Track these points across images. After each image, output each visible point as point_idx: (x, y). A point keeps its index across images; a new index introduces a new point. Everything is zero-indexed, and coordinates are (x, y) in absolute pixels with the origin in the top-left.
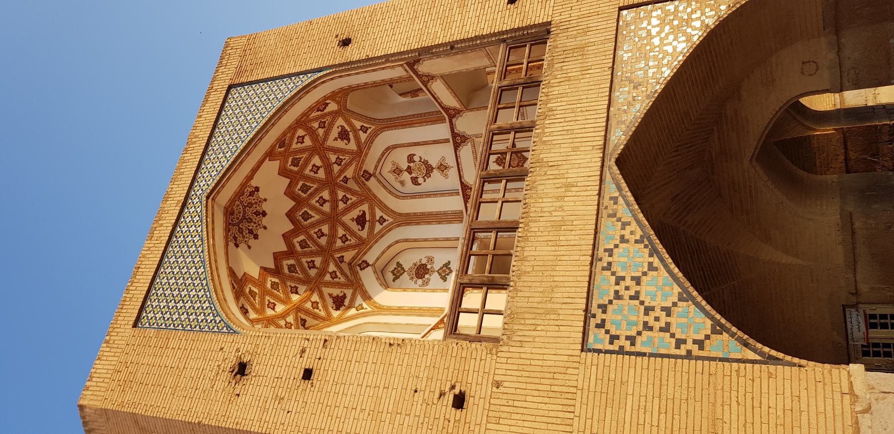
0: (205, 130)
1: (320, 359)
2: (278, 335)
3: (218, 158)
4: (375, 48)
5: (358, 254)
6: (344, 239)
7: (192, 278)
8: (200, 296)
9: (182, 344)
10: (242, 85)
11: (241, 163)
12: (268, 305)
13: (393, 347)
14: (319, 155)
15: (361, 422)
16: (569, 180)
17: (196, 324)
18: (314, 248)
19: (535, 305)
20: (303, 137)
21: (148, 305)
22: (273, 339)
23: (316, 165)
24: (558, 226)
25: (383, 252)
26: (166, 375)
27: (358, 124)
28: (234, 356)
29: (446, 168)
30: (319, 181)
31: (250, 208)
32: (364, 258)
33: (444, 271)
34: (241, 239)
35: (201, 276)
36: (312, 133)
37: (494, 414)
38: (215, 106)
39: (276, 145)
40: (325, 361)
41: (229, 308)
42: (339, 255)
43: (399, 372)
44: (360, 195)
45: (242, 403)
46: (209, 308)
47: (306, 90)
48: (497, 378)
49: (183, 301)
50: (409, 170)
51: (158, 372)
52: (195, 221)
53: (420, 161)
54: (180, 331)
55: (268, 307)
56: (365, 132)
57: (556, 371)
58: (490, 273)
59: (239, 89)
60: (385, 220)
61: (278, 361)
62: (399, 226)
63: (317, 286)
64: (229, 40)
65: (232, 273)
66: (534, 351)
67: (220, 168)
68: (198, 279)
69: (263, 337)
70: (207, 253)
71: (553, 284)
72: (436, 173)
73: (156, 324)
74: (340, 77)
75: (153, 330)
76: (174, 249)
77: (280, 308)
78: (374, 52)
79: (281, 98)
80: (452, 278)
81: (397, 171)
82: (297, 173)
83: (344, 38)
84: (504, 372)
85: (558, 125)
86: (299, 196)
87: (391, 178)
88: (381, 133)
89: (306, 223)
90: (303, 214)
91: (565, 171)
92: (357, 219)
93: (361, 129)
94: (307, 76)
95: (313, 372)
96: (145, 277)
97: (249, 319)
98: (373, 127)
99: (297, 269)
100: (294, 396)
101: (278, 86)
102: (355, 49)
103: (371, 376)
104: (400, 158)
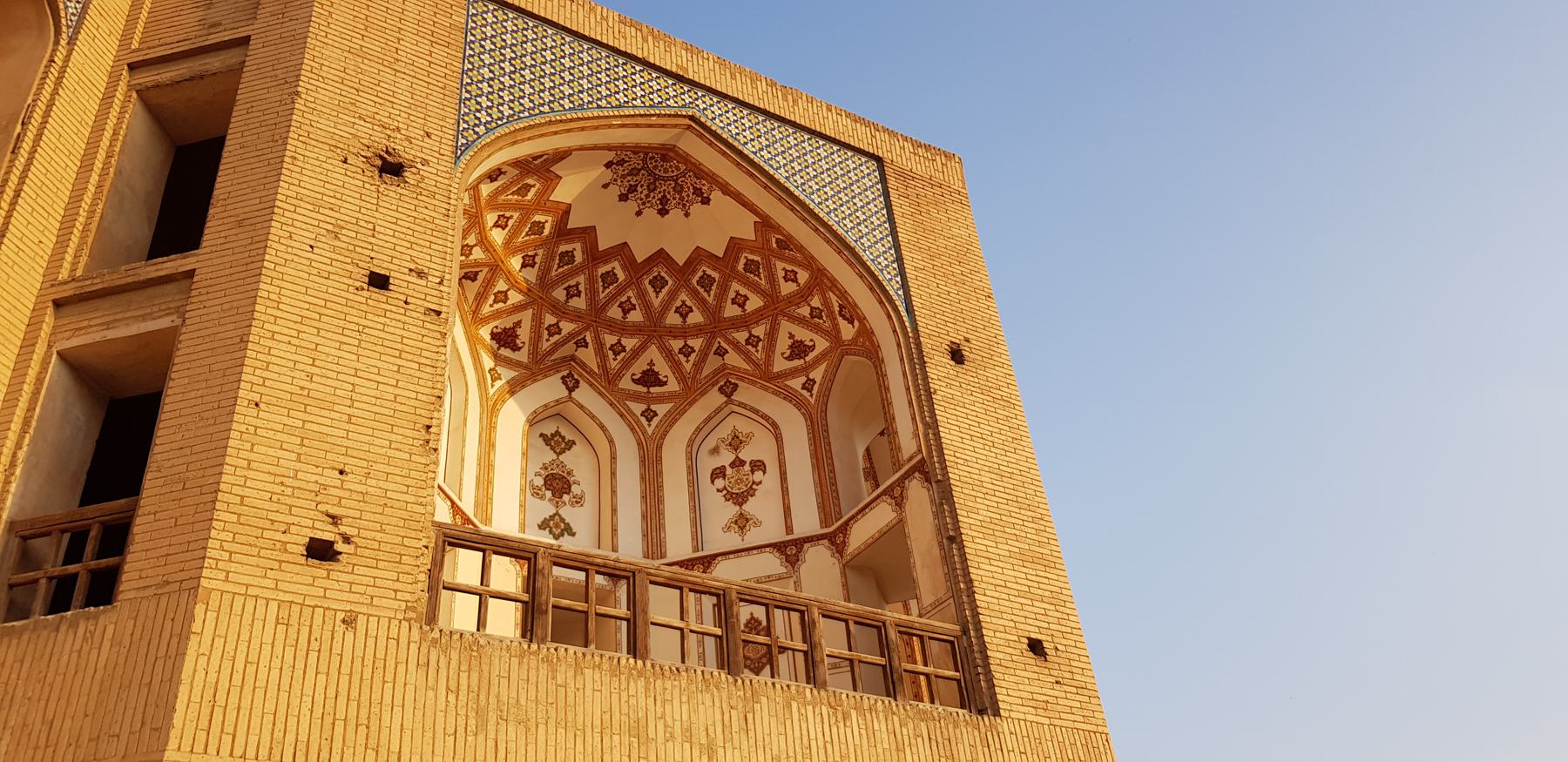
0: (807, 116)
1: (406, 302)
2: (450, 232)
3: (759, 137)
4: (947, 405)
5: (591, 372)
6: (617, 349)
7: (553, 88)
8: (521, 101)
9: (439, 68)
10: (883, 180)
11: (752, 175)
12: (503, 216)
13: (423, 432)
14: (764, 307)
15: (289, 373)
16: (721, 751)
17: (474, 94)
18: (602, 296)
19: (494, 690)
20: (795, 280)
21: (506, 14)
22: (442, 223)
23: (747, 302)
24: (638, 731)
25: (593, 417)
26: (384, 41)
27: (817, 374)
28: (414, 157)
29: (742, 528)
30: (720, 307)
31: (674, 189)
32: (582, 383)
33: (557, 526)
34: (620, 173)
35: (556, 104)
36: (803, 296)
37: (295, 616)
38: (846, 134)
39: (783, 235)
40: (402, 311)
41: (501, 149)
42: (588, 339)
43: (377, 441)
44: (694, 378)
45: (331, 167)
46: (500, 115)
47: (876, 286)
48: (361, 620)
49: (514, 72)
50: (737, 463)
51: (390, 27)
52: (651, 96)
53: (754, 483)
54: (461, 66)
55: (499, 216)
56: (804, 387)
57: (372, 728)
58: (553, 606)
59: (877, 174)
60: (649, 420)
61: (404, 230)
62: (640, 444)
63: (535, 300)
64: (957, 160)
65: (561, 156)
66: (410, 689)
67: (743, 140)
68: (552, 99)
69: (447, 206)
70: (596, 114)
71: (532, 723)
72: (732, 510)
73: (474, 25)
74: (899, 345)
75: (463, 21)
76: (604, 60)
77: (498, 236)
78: (942, 403)
79: (863, 244)
80: (546, 538)
81: (736, 442)
82: (734, 268)
83: (964, 353)
84: (372, 632)
85: (819, 730)
86: (694, 272)
87: (724, 431)
88: (803, 414)
89: (647, 282)
90: (663, 278)
91: (736, 743)
92: (653, 371)
93: (809, 379)
94: (899, 289)
95: (382, 291)
96: (556, 10)
97: (479, 183)
98: (812, 401)
99: (566, 267)
100: (340, 258)
101: (882, 239)
102: (946, 370)
103: (373, 393)
104: (759, 447)
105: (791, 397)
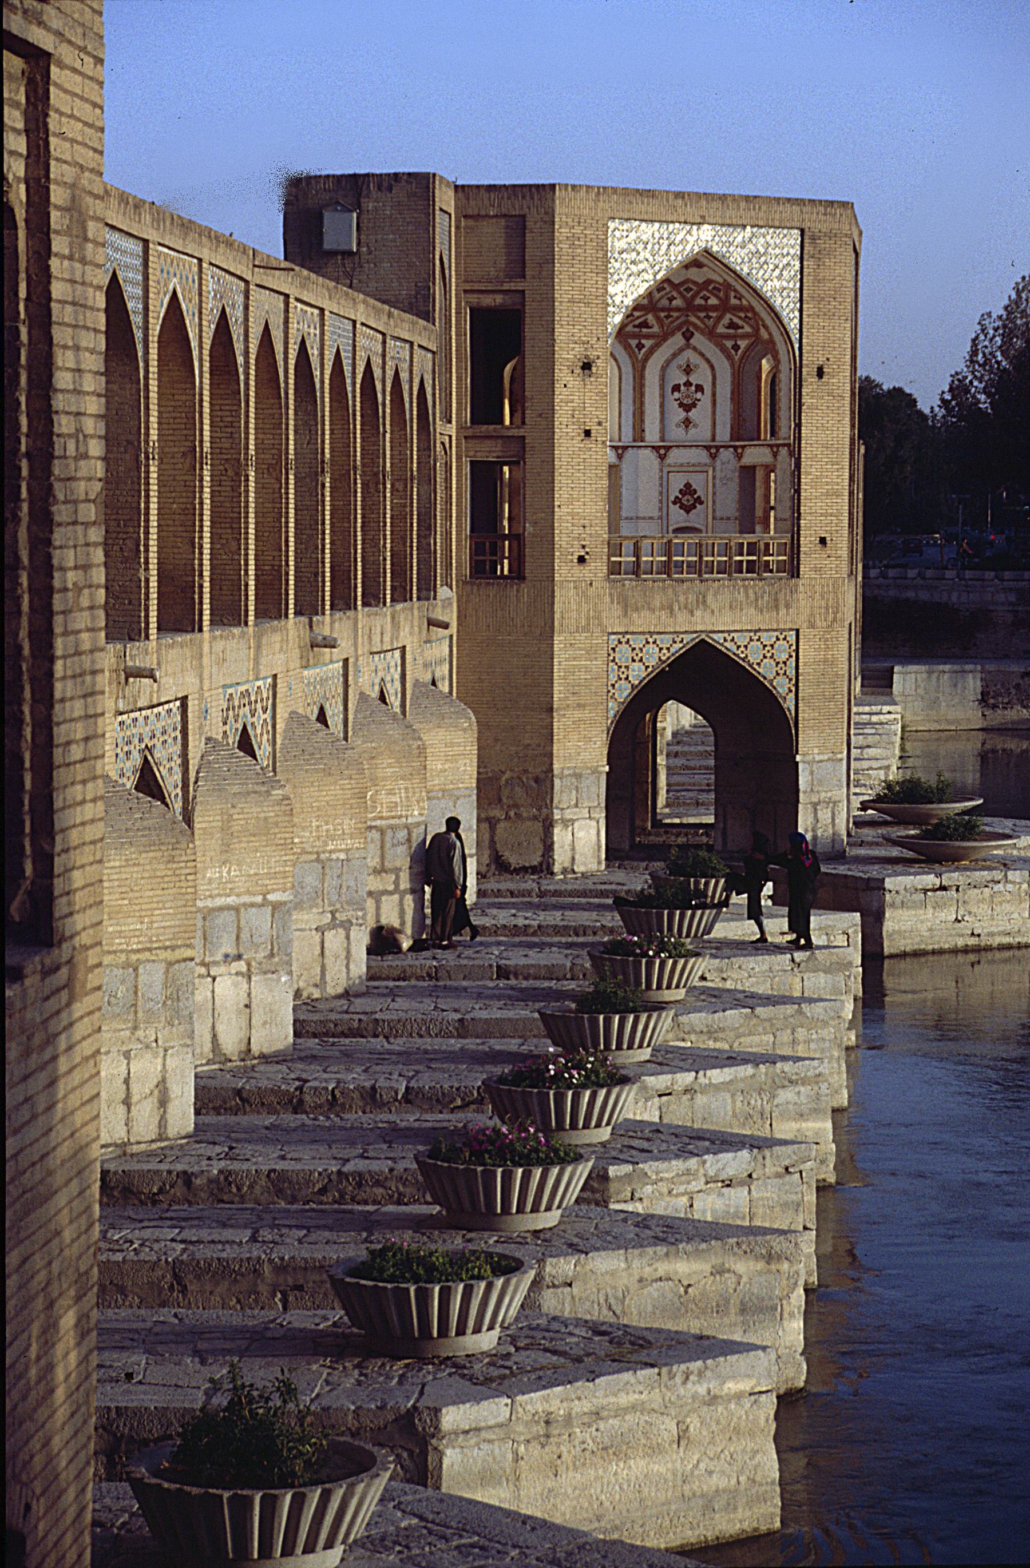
81: (688, 370)
87: (681, 360)
104: (701, 376)
105: (723, 349)
